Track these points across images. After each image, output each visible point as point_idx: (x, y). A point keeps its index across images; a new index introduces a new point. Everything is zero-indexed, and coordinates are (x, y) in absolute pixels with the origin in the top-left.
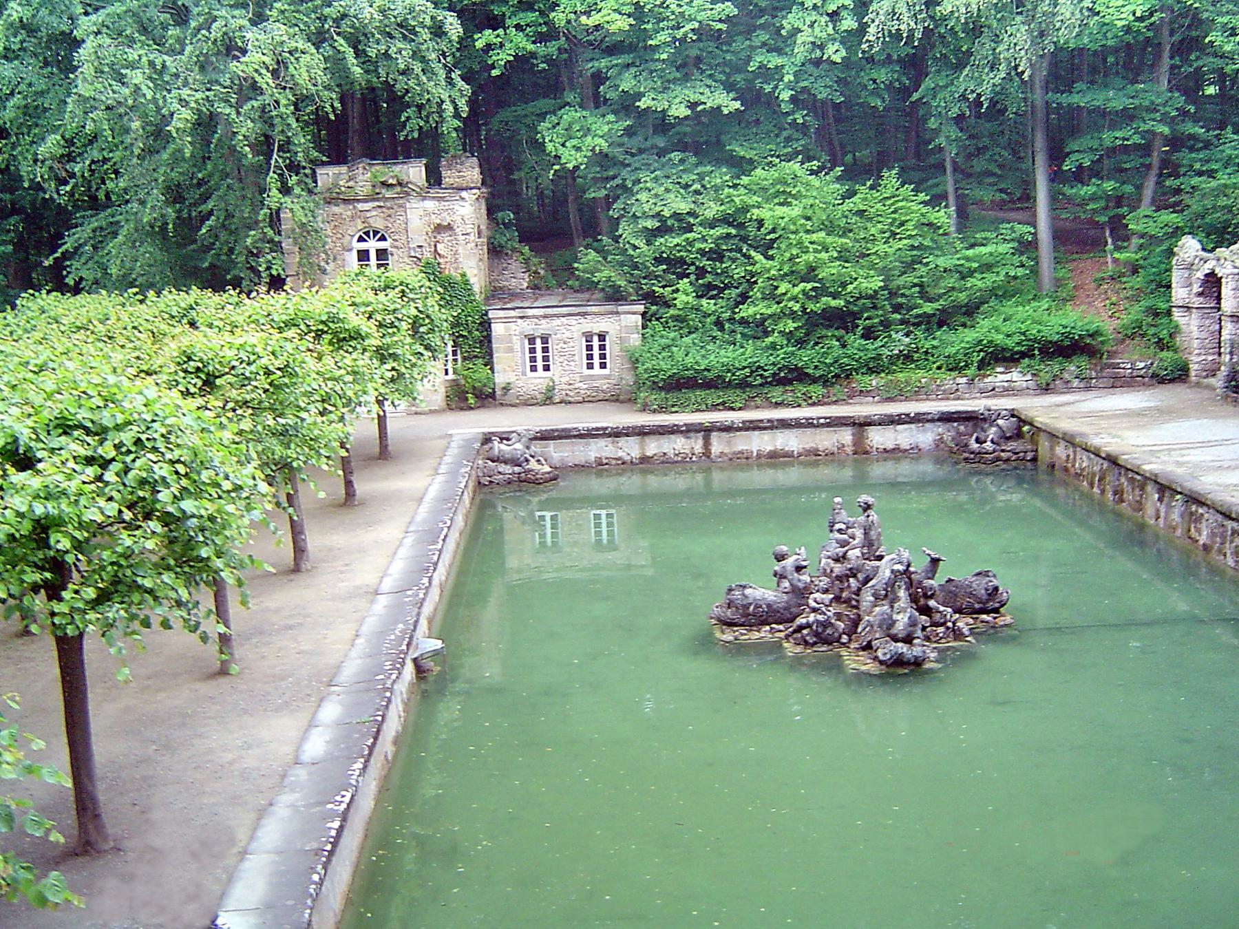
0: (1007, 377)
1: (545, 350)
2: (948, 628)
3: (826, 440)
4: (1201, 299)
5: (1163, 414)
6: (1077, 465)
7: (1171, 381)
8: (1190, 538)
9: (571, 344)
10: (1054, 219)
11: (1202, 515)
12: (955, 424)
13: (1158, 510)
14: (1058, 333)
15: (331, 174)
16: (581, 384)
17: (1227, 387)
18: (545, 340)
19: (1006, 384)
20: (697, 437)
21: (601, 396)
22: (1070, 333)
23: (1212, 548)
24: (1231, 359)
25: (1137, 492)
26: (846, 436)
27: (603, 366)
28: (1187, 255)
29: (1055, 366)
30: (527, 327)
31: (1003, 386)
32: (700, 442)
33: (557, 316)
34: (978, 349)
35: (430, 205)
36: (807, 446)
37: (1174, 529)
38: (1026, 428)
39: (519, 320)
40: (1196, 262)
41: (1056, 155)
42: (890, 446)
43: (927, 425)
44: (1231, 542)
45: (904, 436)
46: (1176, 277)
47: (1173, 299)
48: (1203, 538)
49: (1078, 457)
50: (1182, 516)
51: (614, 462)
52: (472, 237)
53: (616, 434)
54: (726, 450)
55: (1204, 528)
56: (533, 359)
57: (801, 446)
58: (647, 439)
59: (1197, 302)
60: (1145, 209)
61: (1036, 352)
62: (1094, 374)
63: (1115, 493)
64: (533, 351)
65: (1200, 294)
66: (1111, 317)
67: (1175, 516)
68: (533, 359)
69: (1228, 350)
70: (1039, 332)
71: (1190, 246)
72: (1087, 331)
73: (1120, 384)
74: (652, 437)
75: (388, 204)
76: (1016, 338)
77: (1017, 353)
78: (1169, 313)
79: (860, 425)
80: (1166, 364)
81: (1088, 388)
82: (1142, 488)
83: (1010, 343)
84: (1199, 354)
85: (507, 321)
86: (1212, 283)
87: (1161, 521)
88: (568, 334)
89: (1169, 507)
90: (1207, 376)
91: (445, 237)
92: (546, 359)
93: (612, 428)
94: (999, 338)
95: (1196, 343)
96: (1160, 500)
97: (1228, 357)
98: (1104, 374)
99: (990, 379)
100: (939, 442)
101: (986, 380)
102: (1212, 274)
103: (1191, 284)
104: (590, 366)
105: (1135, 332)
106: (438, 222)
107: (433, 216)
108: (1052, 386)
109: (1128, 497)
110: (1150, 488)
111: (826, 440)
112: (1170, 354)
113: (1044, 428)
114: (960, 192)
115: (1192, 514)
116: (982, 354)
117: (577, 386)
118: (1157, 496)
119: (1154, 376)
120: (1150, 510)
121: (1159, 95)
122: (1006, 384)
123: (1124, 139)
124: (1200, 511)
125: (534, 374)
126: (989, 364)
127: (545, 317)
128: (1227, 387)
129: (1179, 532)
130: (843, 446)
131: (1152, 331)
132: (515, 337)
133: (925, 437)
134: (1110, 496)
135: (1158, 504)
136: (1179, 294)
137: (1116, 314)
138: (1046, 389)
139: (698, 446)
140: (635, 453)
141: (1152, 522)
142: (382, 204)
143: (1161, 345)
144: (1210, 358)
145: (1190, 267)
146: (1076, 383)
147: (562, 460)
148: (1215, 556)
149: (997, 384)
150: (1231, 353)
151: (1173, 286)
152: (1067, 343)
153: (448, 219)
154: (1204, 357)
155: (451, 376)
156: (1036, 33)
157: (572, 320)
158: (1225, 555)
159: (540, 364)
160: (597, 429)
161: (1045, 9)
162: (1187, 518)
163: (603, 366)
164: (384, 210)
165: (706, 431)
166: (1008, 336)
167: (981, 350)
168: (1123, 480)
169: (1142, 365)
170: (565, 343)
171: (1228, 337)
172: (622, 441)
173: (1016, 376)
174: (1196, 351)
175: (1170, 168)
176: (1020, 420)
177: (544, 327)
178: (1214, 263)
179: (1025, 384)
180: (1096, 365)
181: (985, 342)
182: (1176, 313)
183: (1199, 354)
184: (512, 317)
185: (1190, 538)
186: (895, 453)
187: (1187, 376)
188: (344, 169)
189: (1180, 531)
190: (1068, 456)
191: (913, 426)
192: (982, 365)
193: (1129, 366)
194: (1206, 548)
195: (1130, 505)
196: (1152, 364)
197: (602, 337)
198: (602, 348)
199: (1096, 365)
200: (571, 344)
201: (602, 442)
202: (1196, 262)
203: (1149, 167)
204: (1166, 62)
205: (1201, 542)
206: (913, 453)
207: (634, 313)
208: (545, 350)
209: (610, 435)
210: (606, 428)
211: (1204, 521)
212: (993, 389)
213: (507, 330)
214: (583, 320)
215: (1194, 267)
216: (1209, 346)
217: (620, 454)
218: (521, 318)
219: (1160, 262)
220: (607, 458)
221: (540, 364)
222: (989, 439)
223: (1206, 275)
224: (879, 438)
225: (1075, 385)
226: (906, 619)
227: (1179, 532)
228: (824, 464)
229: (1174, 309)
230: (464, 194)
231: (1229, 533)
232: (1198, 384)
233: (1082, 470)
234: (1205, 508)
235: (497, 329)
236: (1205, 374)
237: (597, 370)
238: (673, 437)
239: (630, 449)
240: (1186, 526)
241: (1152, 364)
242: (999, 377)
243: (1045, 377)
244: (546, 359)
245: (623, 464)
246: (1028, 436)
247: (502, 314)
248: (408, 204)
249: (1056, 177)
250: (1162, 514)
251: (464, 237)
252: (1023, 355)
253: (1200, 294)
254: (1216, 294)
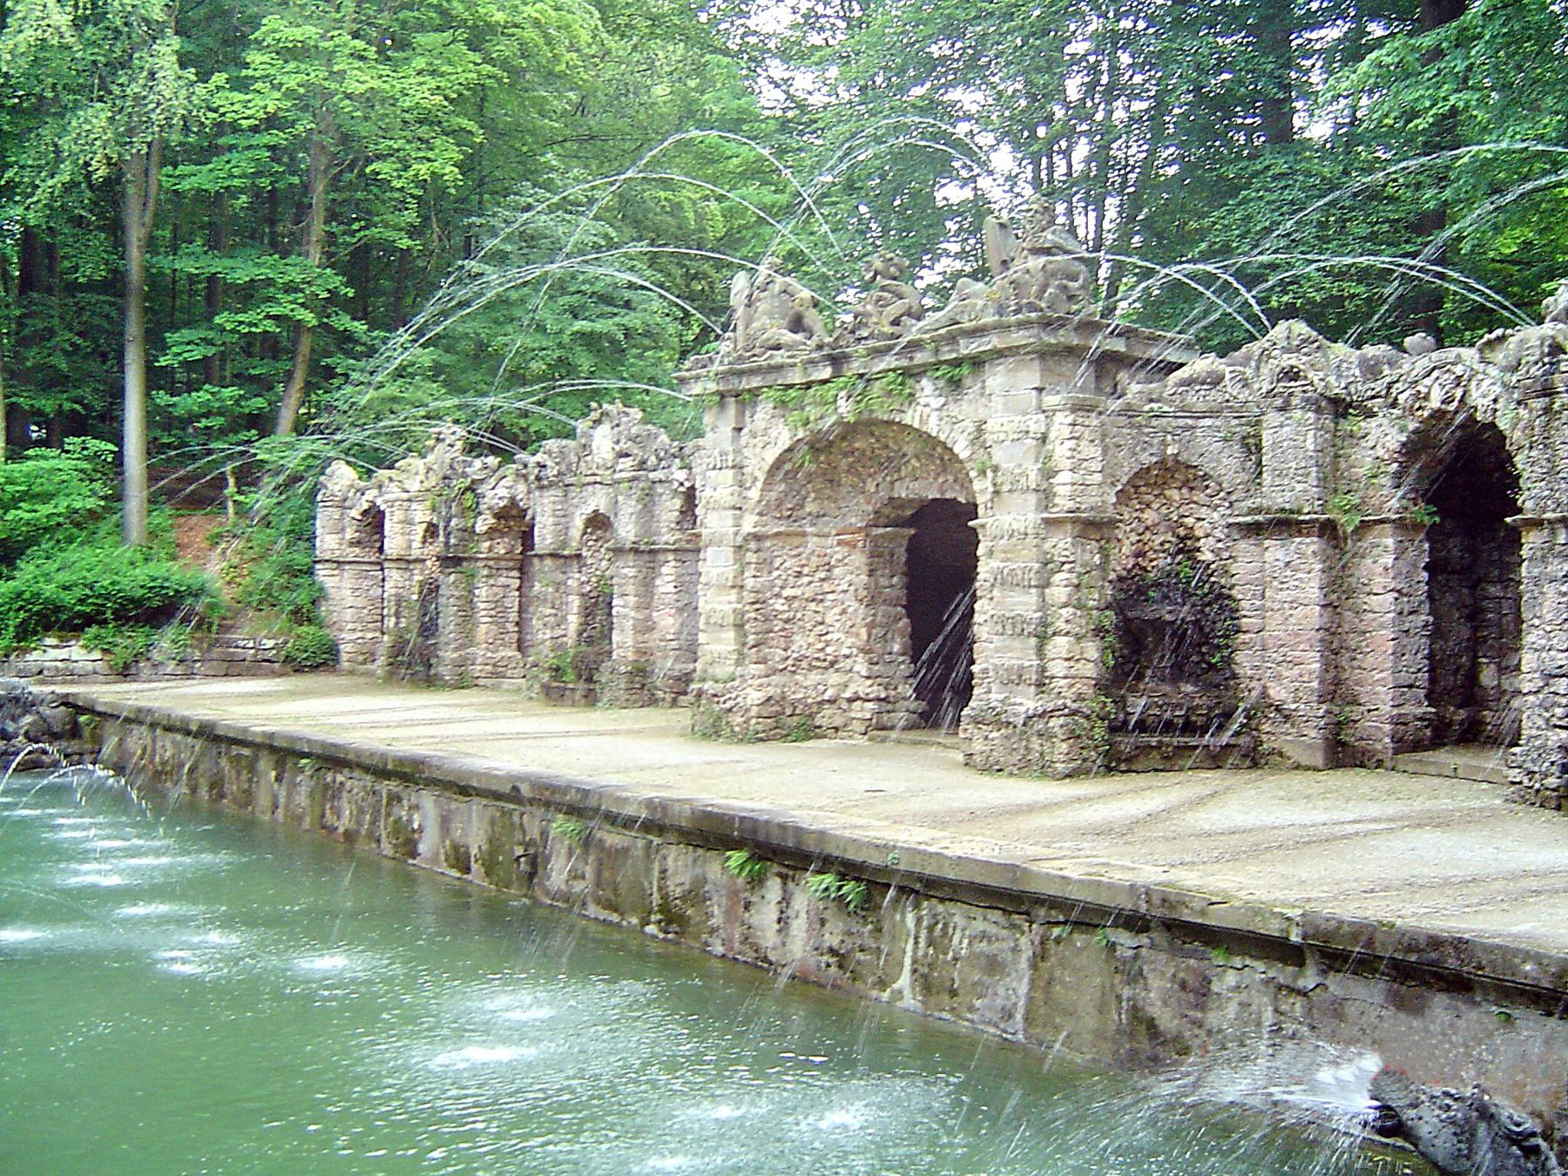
0: (63, 653)
4: (357, 550)
5: (293, 694)
6: (157, 759)
7: (315, 668)
8: (324, 827)
10: (153, 447)
11: (342, 783)
13: (275, 797)
14: (142, 587)
17: (390, 664)
19: (59, 664)
22: (163, 588)
23: (357, 832)
24: (397, 624)
25: (245, 775)
28: (337, 488)
29: (135, 639)
31: (57, 668)
34: (16, 606)
37: (300, 818)
38: (82, 719)
40: (351, 495)
41: (154, 341)
44: (388, 815)
46: (324, 520)
47: (317, 552)
48: (344, 823)
49: (159, 744)
50: (311, 795)
55: (346, 805)
59: (353, 553)
60: (284, 433)
61: (109, 614)
62: (197, 655)
63: (212, 786)
65: (357, 543)
66: (229, 583)
67: (302, 799)
69: (393, 610)
70: (113, 583)
71: (342, 476)
72: (189, 587)
73: (236, 671)
76: (78, 592)
77: (79, 615)
78: (310, 572)
80: (306, 643)
81: (189, 675)
82: (252, 768)
83: (68, 598)
84: (354, 630)
86: (374, 520)
87: (280, 811)
89: (294, 785)
90: (364, 662)
94: (49, 590)
95: (349, 614)
96: (278, 779)
97: (393, 620)
98: (214, 656)
99: (35, 655)
101: (28, 657)
102: (373, 505)
103: (343, 530)
105: (267, 600)
108: (133, 671)
109: (232, 788)
110: (265, 765)
112: (312, 629)
113: (109, 711)
114: (14, 399)
115: (326, 787)
116: (22, 615)
118: (273, 774)
119: (288, 659)
120: (263, 800)
121: (304, 269)
122: (59, 664)
123: (251, 324)
124: (340, 778)
126: (35, 633)
128: (390, 664)
129: (307, 823)
131: (285, 596)
134: (204, 792)
135: (276, 786)
136: (328, 542)
137: (238, 580)
138: (125, 672)
141: (267, 818)
143: (301, 616)
144: (370, 635)
145: (343, 504)
146: (171, 667)
148: (363, 847)
149: (47, 664)
150: (398, 615)
151: (318, 533)
152: (156, 603)
154: (360, 634)
156: (122, 129)
158: (378, 841)
161: (136, 90)
162: (318, 797)
166: (65, 588)
167: (21, 608)
168: (224, 762)
169: (270, 643)
171: (393, 591)
173: (78, 653)
174: (350, 626)
175: (322, 376)
176: (74, 706)
178: (375, 492)
179: (90, 666)
180: (201, 640)
181: (27, 595)
182: (322, 572)
183: (354, 630)
185: (324, 827)
187: (336, 660)
189: (308, 819)
190: (145, 749)
192: (23, 633)
193: (251, 645)
194: (349, 836)
195: (235, 801)
196: (286, 642)
199: (201, 640)
202: (351, 495)
203: (289, 375)
204: (318, 226)
205: (341, 830)
211: (345, 794)
212: (40, 672)
215: (347, 504)
216: (369, 619)
219: (302, 507)
222: (22, 731)
223: (365, 513)
225: (169, 670)
227: (307, 823)
229: (318, 566)
231: (384, 802)
232: (351, 672)
233: (164, 763)
234: (346, 771)
236: (361, 658)
240: (318, 810)
241: (286, 642)
242: (50, 653)
243: (121, 655)
246: (87, 732)
249: (155, 378)
250: (282, 801)
252: (89, 620)
253: (357, 543)
254: (378, 545)
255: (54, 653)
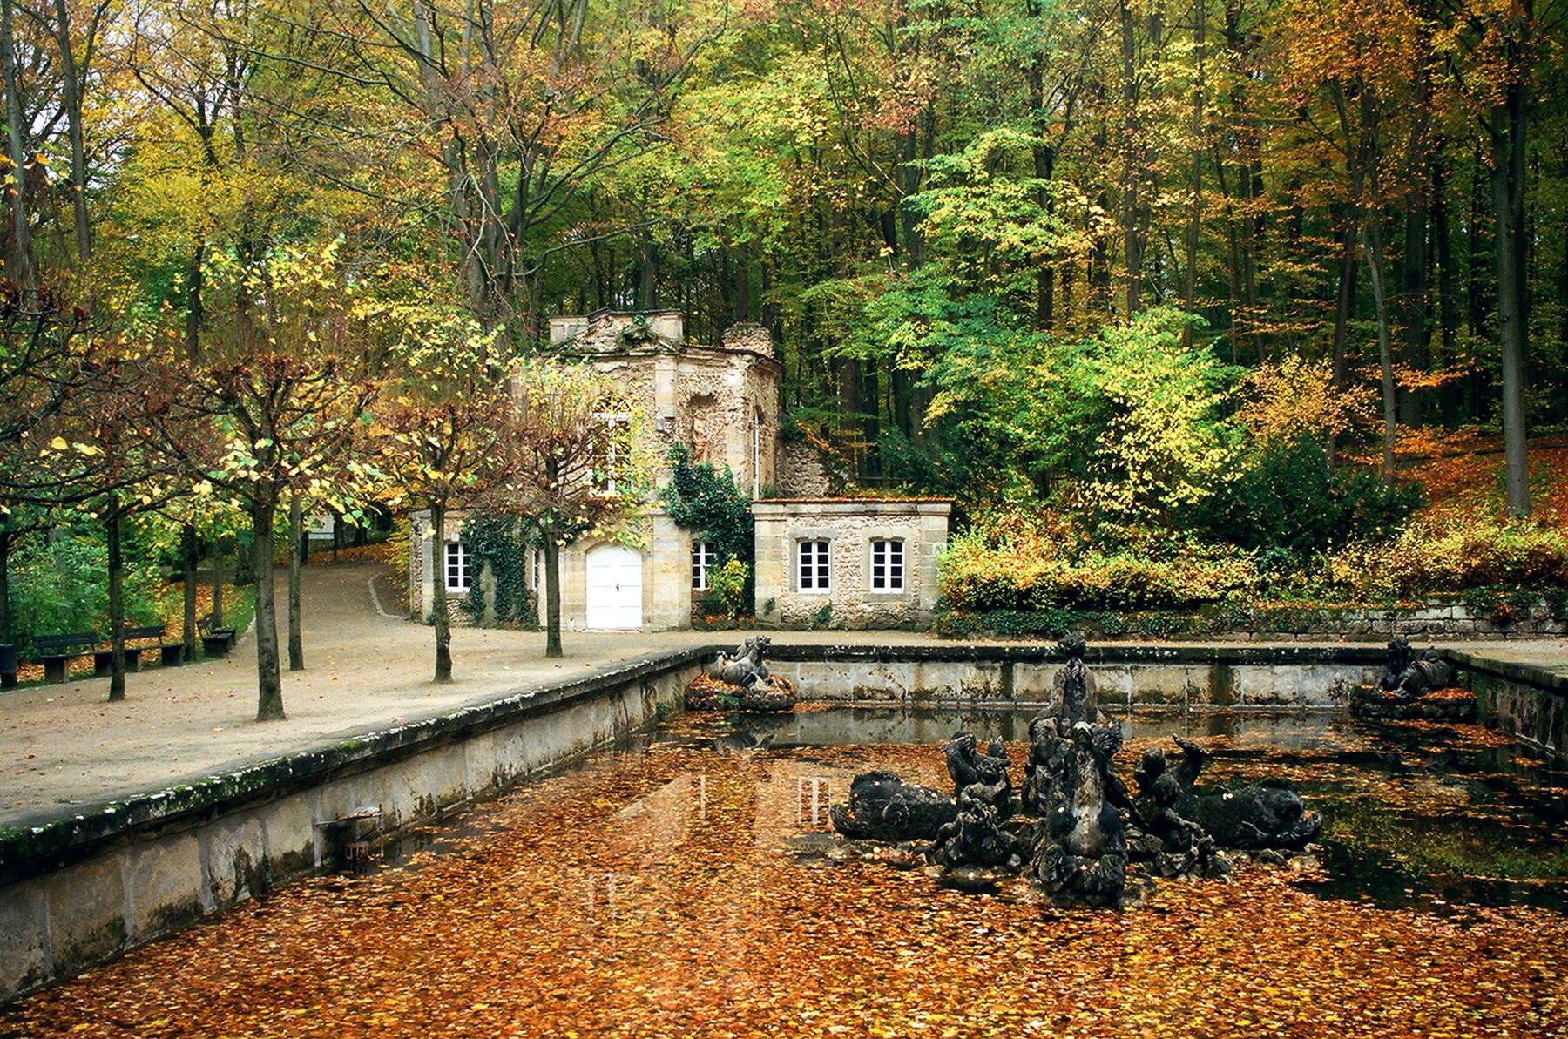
0: (1446, 613)
1: (823, 559)
2: (1191, 855)
3: (1171, 680)
9: (856, 552)
12: (1360, 669)
15: (567, 325)
16: (865, 606)
18: (823, 546)
20: (994, 669)
21: (892, 623)
26: (1200, 676)
27: (896, 583)
30: (802, 528)
32: (997, 675)
33: (840, 515)
35: (688, 369)
36: (1146, 689)
39: (791, 519)
42: (1265, 693)
43: (1320, 668)
45: (1284, 681)
51: (879, 695)
52: (740, 414)
53: (884, 656)
54: (1034, 688)
56: (806, 571)
57: (1137, 688)
58: (927, 667)
64: (806, 560)
68: (806, 571)
74: (933, 664)
75: (634, 365)
79: (1224, 663)
85: (775, 518)
88: (851, 540)
91: (709, 413)
92: (823, 571)
93: (877, 648)
100: (1336, 693)
104: (879, 583)
106: (697, 390)
107: (690, 383)
111: (1171, 680)
117: (859, 607)
125: (807, 590)
127: (824, 515)
130: (1198, 691)
132: (784, 541)
133: (1316, 684)
139: (995, 681)
140: (909, 685)
142: (625, 364)
147: (811, 689)
153: (710, 389)
155: (702, 588)
157: (858, 521)
159: (815, 577)
160: (858, 649)
163: (896, 583)
164: (629, 372)
165: (1007, 660)
170: (847, 550)
172: (894, 668)
177: (821, 529)
184: (782, 515)
186: (1273, 709)
188: (583, 321)
191: (1298, 668)
197: (897, 546)
198: (897, 559)
200: (856, 552)
201: (865, 668)
206: (1303, 712)
207: (938, 514)
208: (823, 559)
209: (875, 659)
210: (871, 648)
213: (774, 530)
214: (872, 521)
217: (889, 684)
218: (793, 515)
220: (869, 690)
221: (815, 577)
224: (1250, 680)
226: (1094, 819)
228: (1169, 718)
230: (734, 359)
235: (762, 529)
237: (888, 589)
238: (961, 666)
239: (903, 678)
244: (823, 571)
245: (891, 698)
247: (767, 509)
248: (657, 366)
251: (730, 414)
255: (1435, 613)
